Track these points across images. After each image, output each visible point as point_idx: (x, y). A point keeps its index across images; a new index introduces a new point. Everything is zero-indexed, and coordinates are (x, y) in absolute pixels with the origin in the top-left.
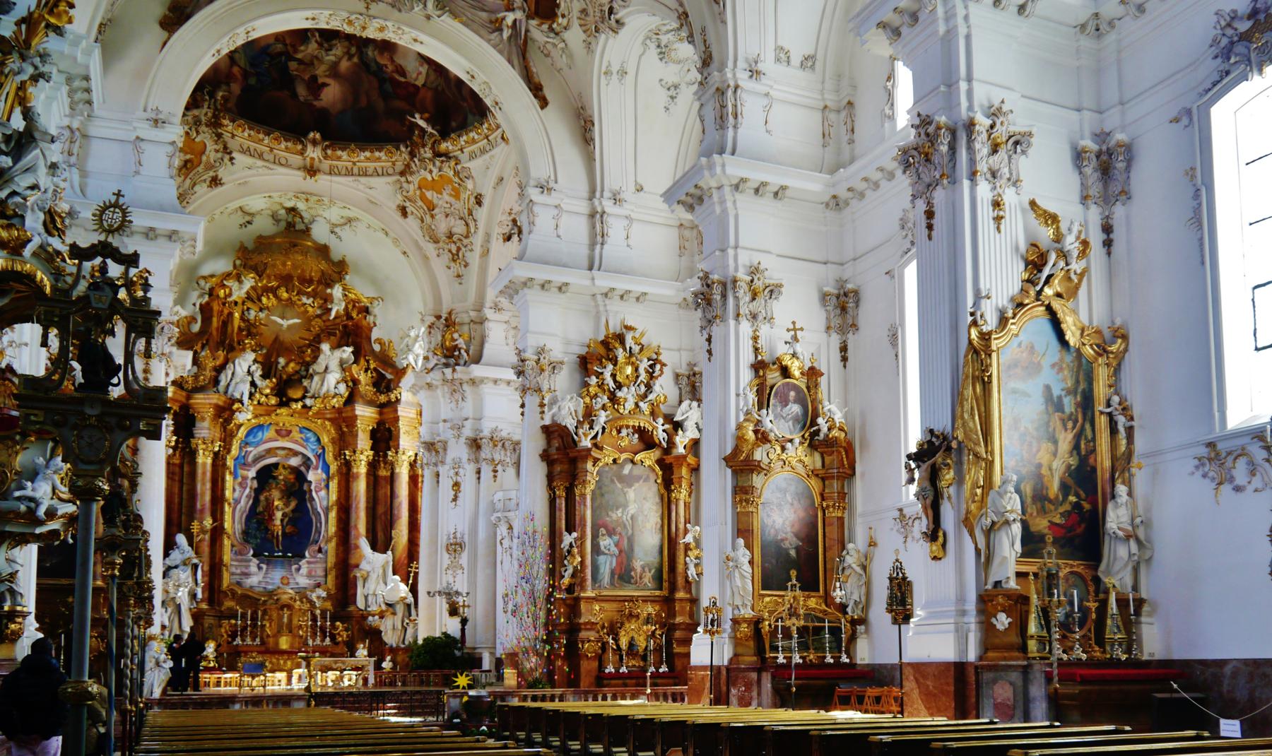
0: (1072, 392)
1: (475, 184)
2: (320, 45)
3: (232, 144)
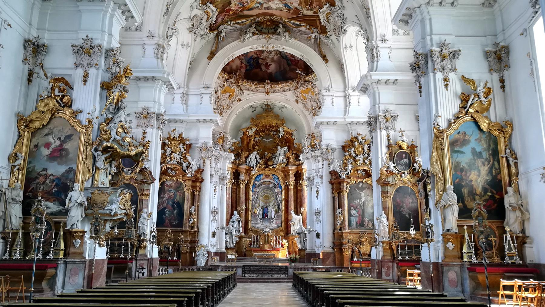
0: (488, 149)
3: (243, 88)
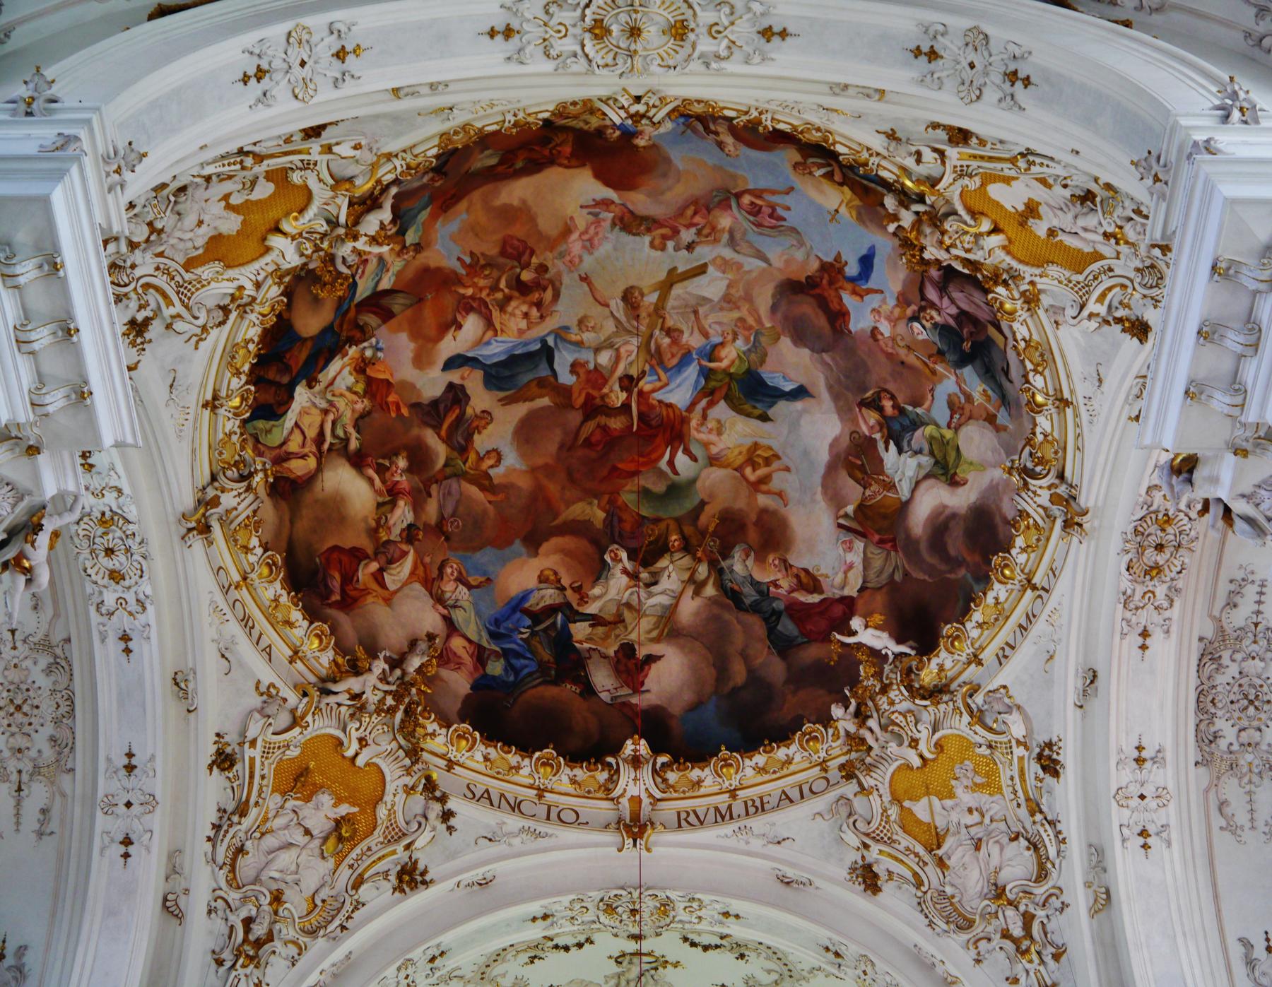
1: (1027, 719)
2: (634, 576)
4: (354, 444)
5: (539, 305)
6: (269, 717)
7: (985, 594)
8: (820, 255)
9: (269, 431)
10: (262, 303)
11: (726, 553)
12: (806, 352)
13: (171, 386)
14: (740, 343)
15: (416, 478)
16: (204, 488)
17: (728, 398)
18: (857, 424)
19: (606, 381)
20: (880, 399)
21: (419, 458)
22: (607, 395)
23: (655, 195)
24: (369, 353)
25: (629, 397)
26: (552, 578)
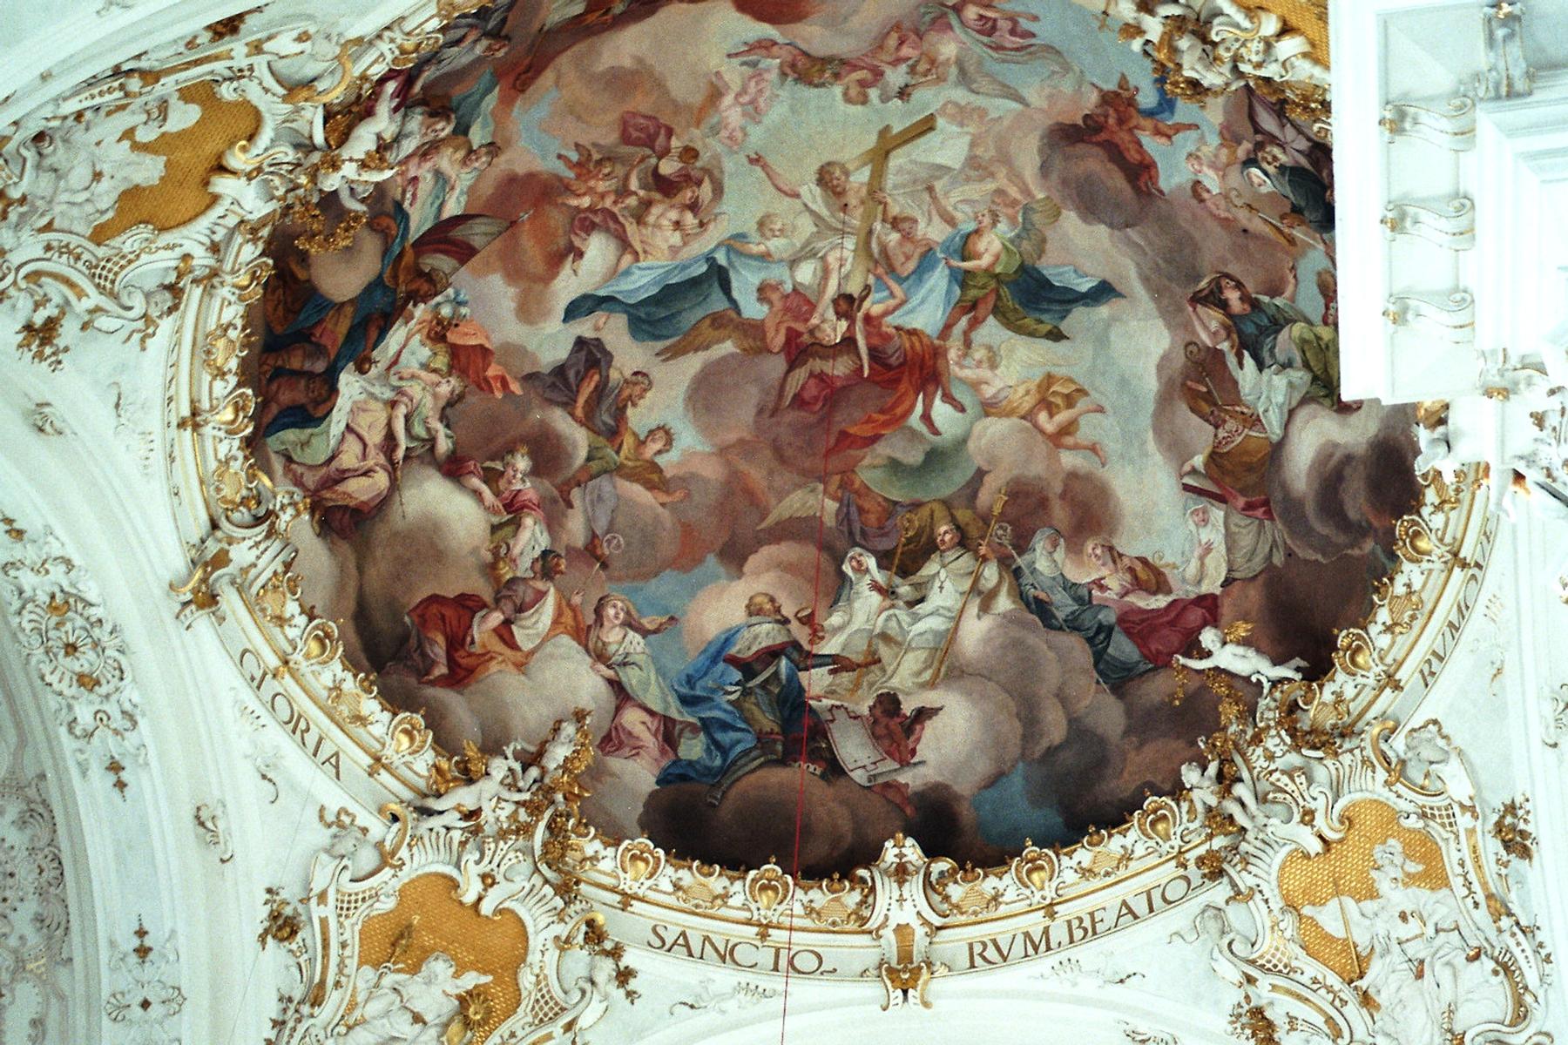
1: (1471, 771)
2: (888, 592)
4: (444, 445)
5: (694, 207)
6: (343, 857)
7: (1391, 579)
8: (1095, 80)
9: (305, 444)
10: (233, 272)
11: (1022, 543)
12: (1102, 230)
13: (117, 406)
14: (1002, 226)
15: (547, 483)
16: (203, 541)
17: (997, 311)
18: (1194, 332)
19: (813, 307)
20: (1221, 291)
21: (547, 454)
22: (817, 327)
23: (835, 23)
24: (446, 311)
25: (851, 328)
26: (768, 606)
